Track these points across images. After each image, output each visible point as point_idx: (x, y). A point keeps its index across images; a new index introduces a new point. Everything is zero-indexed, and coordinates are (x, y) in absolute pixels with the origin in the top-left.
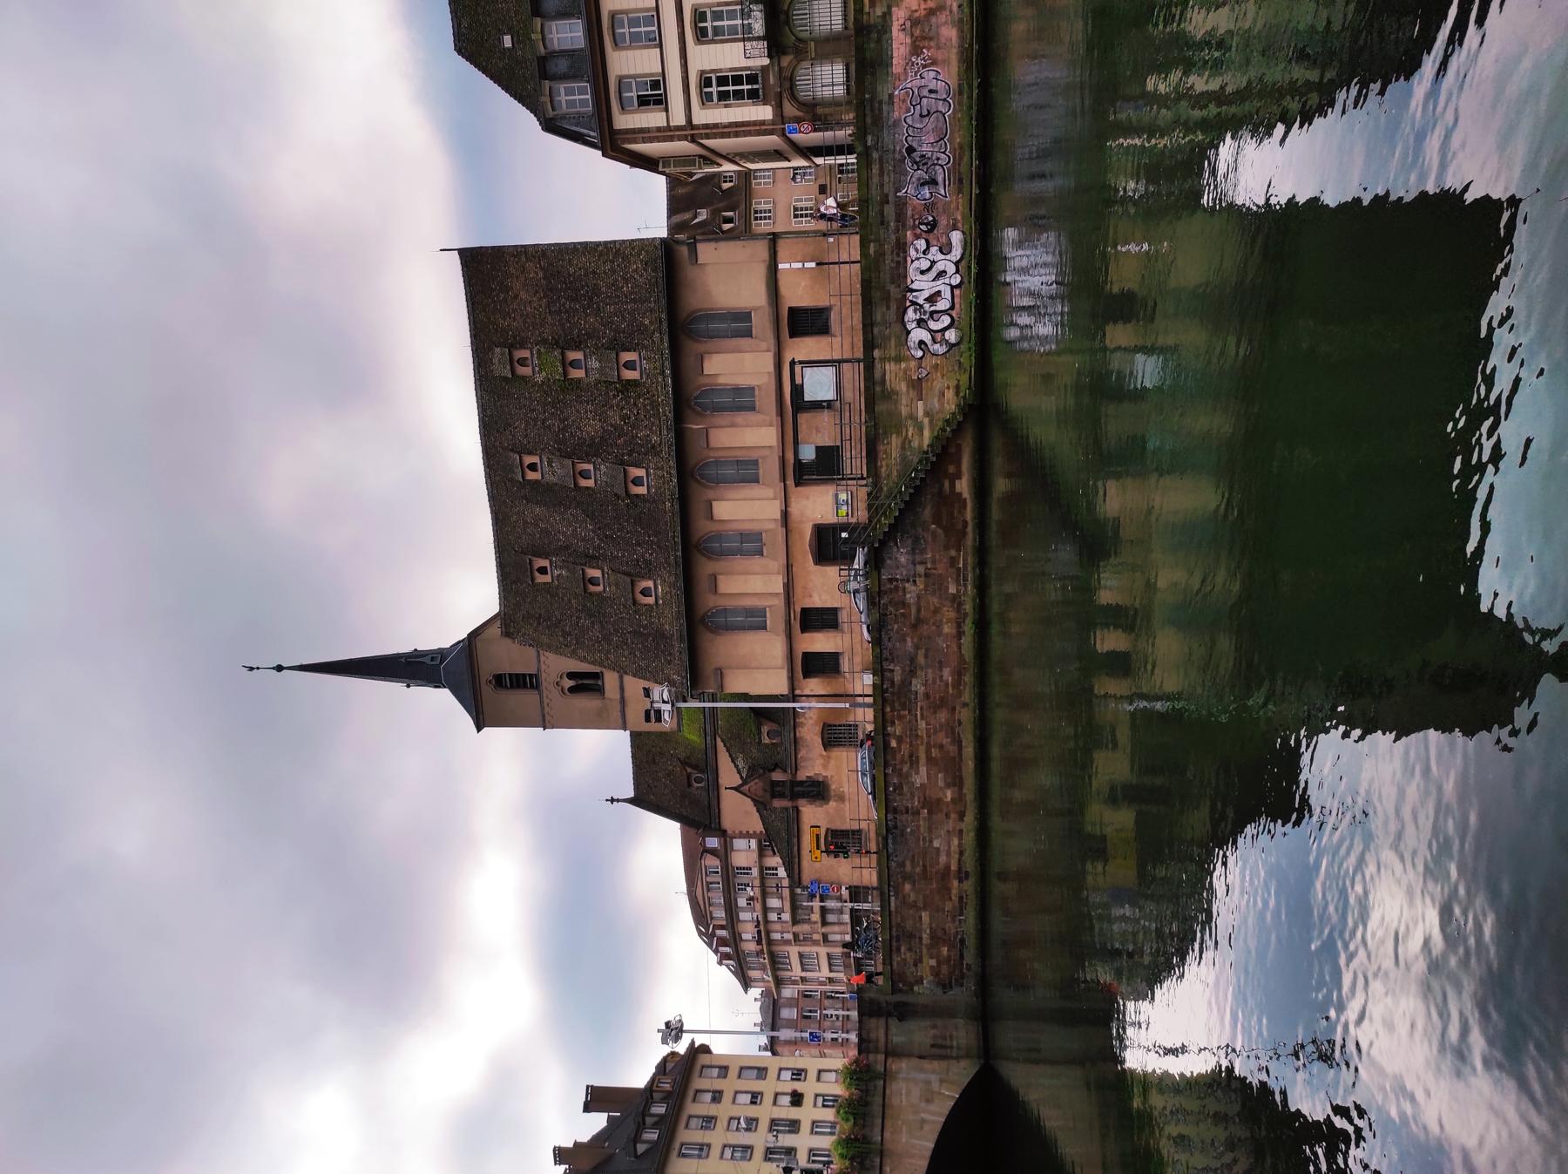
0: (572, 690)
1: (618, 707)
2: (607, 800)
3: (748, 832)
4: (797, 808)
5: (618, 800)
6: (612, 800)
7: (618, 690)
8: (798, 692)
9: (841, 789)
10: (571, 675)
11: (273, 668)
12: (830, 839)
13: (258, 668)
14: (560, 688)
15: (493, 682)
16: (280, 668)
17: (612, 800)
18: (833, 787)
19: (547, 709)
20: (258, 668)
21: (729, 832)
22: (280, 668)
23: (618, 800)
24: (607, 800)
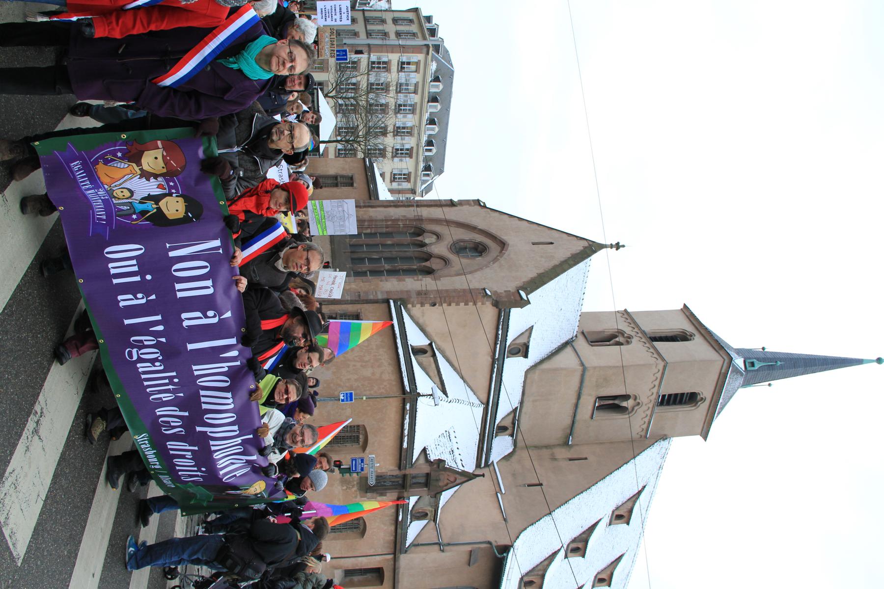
0: (626, 397)
1: (585, 391)
2: (623, 246)
3: (466, 304)
4: (400, 468)
5: (611, 246)
6: (618, 246)
7: (580, 406)
8: (391, 556)
9: (345, 488)
10: (623, 410)
12: (361, 436)
14: (638, 400)
15: (699, 397)
17: (618, 246)
18: (355, 488)
19: (657, 383)
21: (488, 304)
23: (611, 246)
24: (623, 246)
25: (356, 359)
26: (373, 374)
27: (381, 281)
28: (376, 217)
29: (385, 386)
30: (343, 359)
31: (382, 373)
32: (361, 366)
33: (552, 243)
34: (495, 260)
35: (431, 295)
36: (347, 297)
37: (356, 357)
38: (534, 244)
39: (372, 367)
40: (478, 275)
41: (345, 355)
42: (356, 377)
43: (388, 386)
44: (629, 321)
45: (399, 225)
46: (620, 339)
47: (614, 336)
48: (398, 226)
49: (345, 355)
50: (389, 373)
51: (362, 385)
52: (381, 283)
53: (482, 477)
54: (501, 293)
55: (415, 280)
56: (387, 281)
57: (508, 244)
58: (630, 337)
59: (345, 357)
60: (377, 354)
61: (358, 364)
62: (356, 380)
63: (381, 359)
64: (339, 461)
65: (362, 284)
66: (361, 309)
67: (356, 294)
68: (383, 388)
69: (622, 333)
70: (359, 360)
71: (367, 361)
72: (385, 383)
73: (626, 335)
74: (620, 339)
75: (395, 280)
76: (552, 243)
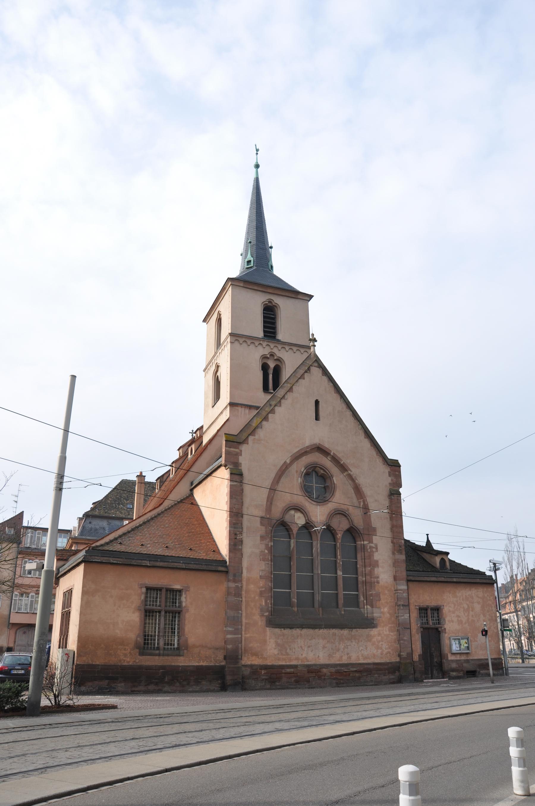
11: (257, 162)
13: (257, 154)
16: (257, 166)
20: (257, 154)
22: (257, 166)
25: (466, 614)
26: (479, 603)
27: (378, 582)
28: (262, 570)
29: (488, 595)
30: (467, 625)
31: (477, 596)
32: (472, 611)
33: (317, 402)
34: (343, 468)
35: (401, 542)
36: (406, 617)
37: (464, 614)
38: (317, 418)
39: (473, 603)
40: (367, 491)
41: (464, 622)
42: (482, 616)
43: (488, 594)
44: (249, 342)
45: (271, 546)
46: (272, 364)
47: (265, 368)
48: (272, 547)
49: (464, 622)
50: (478, 591)
51: (488, 612)
52: (381, 583)
53: (429, 536)
54: (392, 480)
55: (377, 551)
56: (378, 577)
57: (319, 444)
58: (272, 355)
59: (465, 623)
60: (461, 598)
61: (471, 613)
62: (484, 616)
63: (466, 596)
64: (482, 632)
65: (383, 601)
66: (416, 606)
67: (402, 608)
68: (490, 597)
69: (264, 357)
70: (467, 612)
71: (468, 606)
72: (486, 595)
73: (268, 356)
74: (272, 364)
75: (376, 569)
76: (317, 402)
